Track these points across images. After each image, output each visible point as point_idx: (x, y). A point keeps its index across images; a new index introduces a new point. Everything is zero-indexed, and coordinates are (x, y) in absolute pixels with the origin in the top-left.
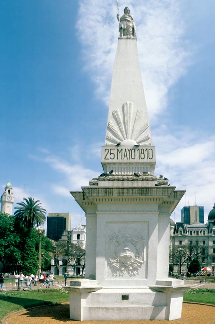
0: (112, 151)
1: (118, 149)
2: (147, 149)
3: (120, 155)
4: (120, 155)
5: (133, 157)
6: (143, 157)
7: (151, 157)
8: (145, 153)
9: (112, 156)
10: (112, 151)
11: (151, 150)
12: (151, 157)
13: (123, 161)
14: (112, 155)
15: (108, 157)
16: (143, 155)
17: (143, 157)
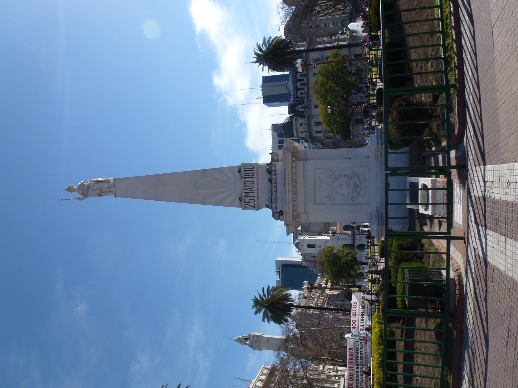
0: (247, 201)
1: (245, 196)
2: (245, 171)
3: (250, 194)
4: (250, 194)
5: (252, 183)
6: (252, 174)
7: (252, 167)
8: (248, 172)
9: (252, 201)
10: (247, 201)
11: (245, 167)
12: (252, 167)
13: (256, 192)
14: (250, 201)
15: (252, 204)
16: (250, 174)
17: (252, 174)
